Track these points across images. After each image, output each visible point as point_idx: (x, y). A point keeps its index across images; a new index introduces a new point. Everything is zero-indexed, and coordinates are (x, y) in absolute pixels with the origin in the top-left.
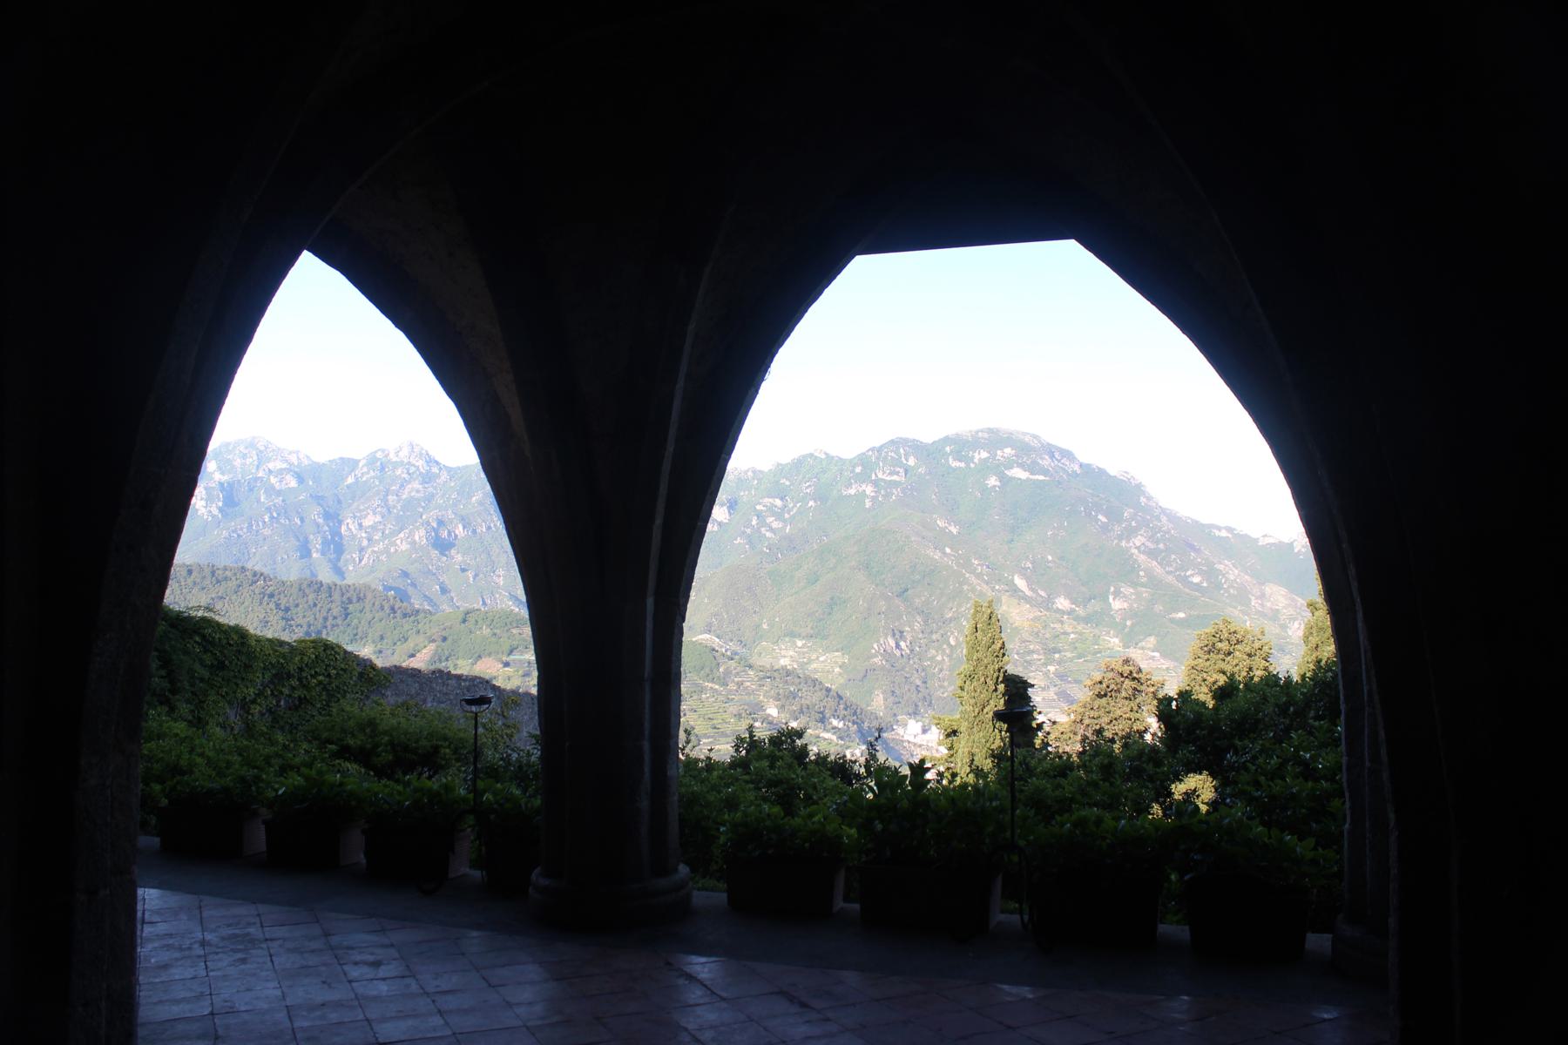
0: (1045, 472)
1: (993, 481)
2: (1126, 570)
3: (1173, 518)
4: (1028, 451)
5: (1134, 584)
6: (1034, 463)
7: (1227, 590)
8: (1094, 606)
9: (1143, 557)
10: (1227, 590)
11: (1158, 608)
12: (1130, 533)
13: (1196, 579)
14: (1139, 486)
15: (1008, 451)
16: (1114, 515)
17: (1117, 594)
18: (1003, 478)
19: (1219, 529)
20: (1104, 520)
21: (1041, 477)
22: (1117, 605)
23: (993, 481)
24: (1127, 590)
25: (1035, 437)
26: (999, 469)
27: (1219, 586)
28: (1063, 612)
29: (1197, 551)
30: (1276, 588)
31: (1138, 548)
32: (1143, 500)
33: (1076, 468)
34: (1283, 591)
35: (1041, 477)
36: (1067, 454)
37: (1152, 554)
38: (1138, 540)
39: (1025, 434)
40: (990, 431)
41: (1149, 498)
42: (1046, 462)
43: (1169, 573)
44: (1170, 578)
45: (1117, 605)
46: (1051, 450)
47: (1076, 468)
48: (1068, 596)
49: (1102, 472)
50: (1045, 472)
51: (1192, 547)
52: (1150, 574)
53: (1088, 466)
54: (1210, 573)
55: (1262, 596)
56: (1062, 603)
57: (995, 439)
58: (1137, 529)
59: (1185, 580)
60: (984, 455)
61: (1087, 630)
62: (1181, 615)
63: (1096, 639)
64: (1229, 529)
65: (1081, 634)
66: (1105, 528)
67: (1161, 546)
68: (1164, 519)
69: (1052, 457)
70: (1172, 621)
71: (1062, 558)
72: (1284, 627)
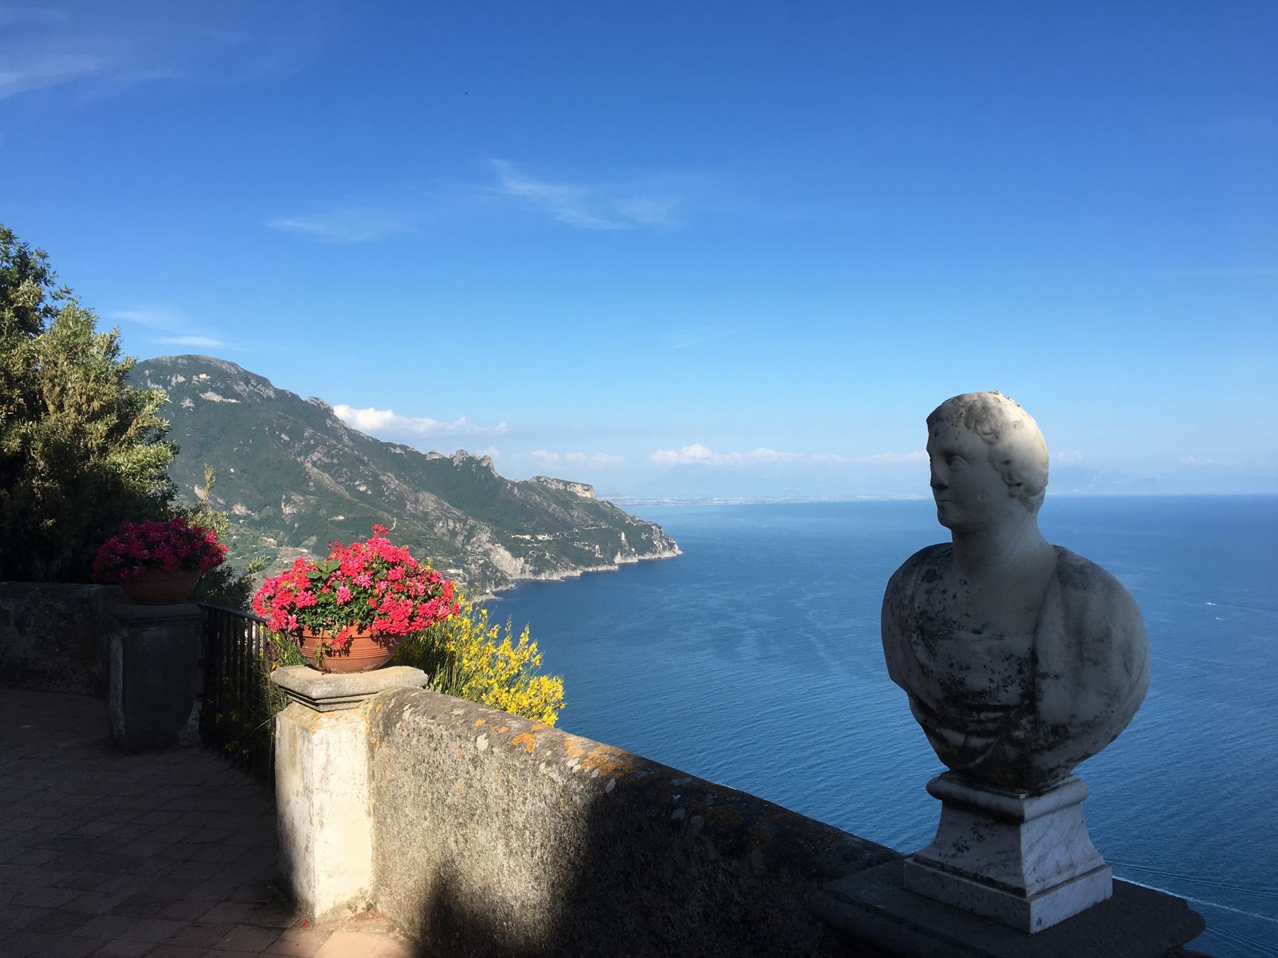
0: (237, 396)
1: (187, 403)
2: (299, 481)
3: (355, 436)
4: (223, 376)
5: (303, 493)
6: (229, 388)
7: (388, 497)
8: (269, 511)
9: (315, 470)
10: (388, 497)
11: (323, 512)
12: (309, 450)
13: (363, 489)
14: (328, 412)
15: (203, 376)
16: (296, 435)
17: (288, 501)
18: (196, 399)
19: (395, 446)
20: (287, 438)
21: (233, 401)
22: (287, 510)
23: (187, 403)
24: (297, 498)
25: (232, 365)
26: (193, 392)
27: (381, 493)
28: (239, 517)
29: (366, 465)
30: (427, 495)
31: (314, 464)
32: (329, 422)
33: (271, 393)
34: (433, 497)
35: (233, 401)
36: (264, 382)
37: (325, 468)
38: (315, 456)
39: (223, 362)
40: (190, 357)
41: (336, 420)
42: (240, 388)
43: (340, 483)
44: (340, 489)
45: (287, 510)
46: (247, 377)
47: (271, 393)
48: (245, 503)
49: (295, 398)
50: (237, 396)
51: (362, 462)
52: (318, 484)
53: (283, 391)
54: (375, 483)
55: (417, 500)
56: (240, 509)
57: (194, 364)
58: (315, 446)
59: (352, 490)
60: (181, 379)
61: (249, 533)
62: (341, 518)
63: (256, 538)
64: (403, 447)
65: (242, 535)
66: (286, 444)
67: (335, 461)
68: (346, 439)
69: (247, 382)
70: (332, 522)
71: (243, 471)
72: (431, 526)
